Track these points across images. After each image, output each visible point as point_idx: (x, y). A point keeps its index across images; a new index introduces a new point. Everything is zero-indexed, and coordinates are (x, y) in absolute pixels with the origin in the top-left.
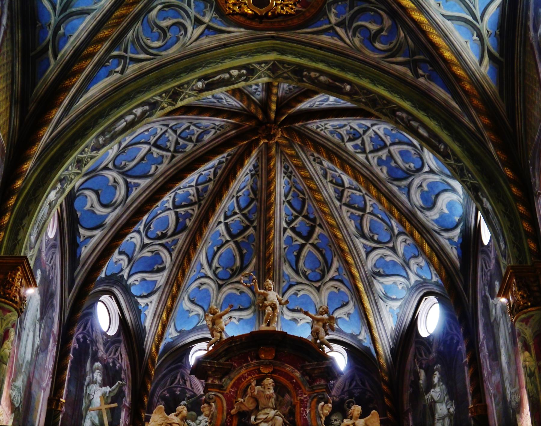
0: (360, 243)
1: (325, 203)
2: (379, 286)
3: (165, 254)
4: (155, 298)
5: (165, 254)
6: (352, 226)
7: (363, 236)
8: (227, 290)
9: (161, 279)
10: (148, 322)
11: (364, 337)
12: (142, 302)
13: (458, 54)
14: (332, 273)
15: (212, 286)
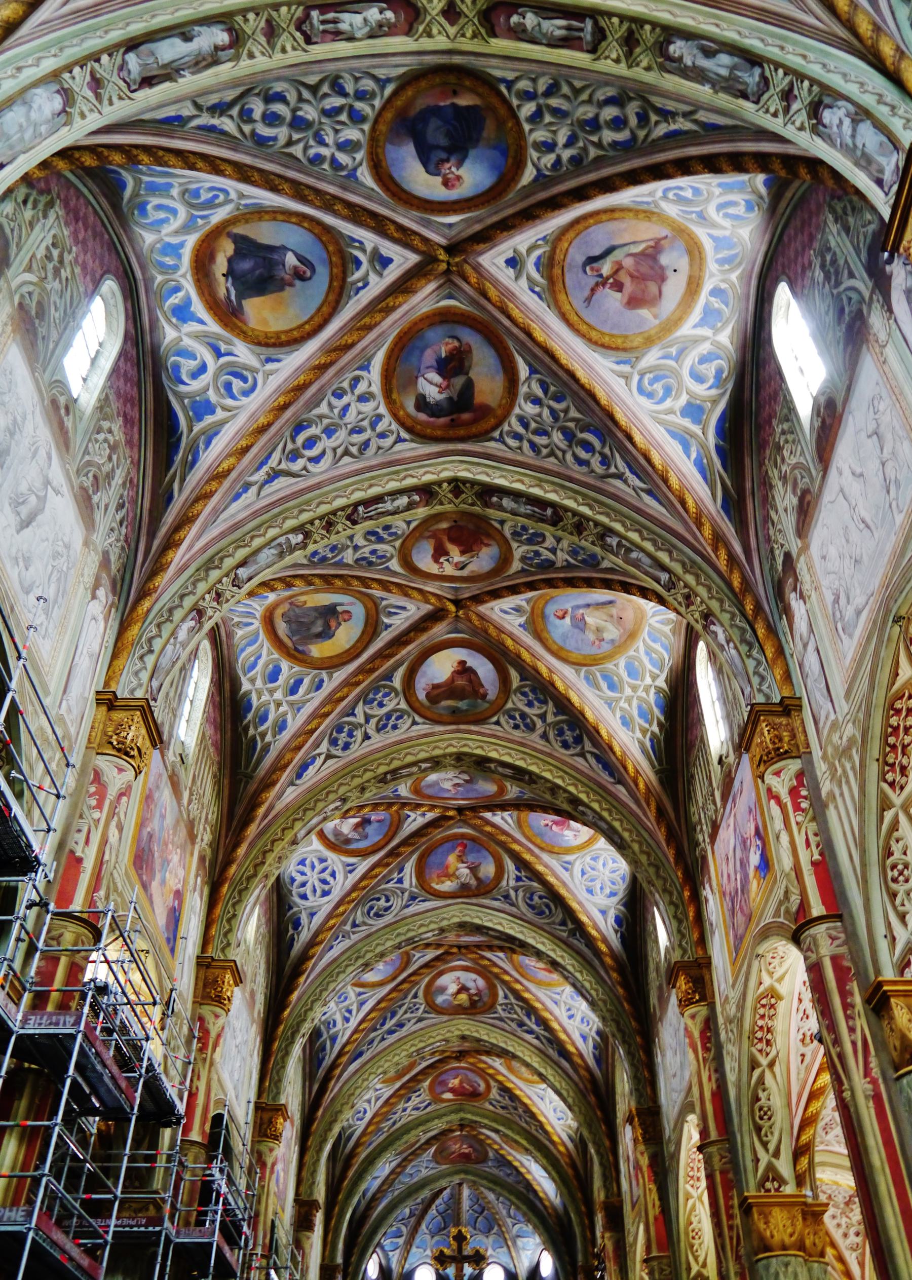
0: (509, 1221)
1: (489, 1202)
2: (520, 1242)
3: (404, 1229)
4: (398, 1251)
5: (404, 1229)
6: (504, 1212)
7: (510, 1217)
8: (436, 1238)
9: (401, 1241)
10: (394, 1265)
11: (512, 1266)
12: (391, 1254)
13: (546, 1194)
14: (495, 1230)
15: (428, 1237)
